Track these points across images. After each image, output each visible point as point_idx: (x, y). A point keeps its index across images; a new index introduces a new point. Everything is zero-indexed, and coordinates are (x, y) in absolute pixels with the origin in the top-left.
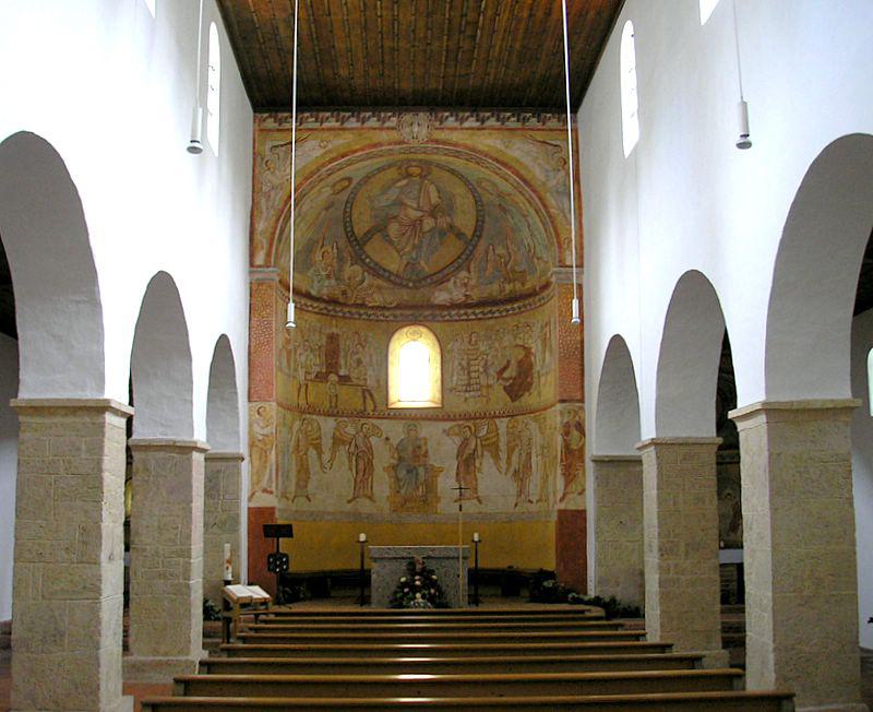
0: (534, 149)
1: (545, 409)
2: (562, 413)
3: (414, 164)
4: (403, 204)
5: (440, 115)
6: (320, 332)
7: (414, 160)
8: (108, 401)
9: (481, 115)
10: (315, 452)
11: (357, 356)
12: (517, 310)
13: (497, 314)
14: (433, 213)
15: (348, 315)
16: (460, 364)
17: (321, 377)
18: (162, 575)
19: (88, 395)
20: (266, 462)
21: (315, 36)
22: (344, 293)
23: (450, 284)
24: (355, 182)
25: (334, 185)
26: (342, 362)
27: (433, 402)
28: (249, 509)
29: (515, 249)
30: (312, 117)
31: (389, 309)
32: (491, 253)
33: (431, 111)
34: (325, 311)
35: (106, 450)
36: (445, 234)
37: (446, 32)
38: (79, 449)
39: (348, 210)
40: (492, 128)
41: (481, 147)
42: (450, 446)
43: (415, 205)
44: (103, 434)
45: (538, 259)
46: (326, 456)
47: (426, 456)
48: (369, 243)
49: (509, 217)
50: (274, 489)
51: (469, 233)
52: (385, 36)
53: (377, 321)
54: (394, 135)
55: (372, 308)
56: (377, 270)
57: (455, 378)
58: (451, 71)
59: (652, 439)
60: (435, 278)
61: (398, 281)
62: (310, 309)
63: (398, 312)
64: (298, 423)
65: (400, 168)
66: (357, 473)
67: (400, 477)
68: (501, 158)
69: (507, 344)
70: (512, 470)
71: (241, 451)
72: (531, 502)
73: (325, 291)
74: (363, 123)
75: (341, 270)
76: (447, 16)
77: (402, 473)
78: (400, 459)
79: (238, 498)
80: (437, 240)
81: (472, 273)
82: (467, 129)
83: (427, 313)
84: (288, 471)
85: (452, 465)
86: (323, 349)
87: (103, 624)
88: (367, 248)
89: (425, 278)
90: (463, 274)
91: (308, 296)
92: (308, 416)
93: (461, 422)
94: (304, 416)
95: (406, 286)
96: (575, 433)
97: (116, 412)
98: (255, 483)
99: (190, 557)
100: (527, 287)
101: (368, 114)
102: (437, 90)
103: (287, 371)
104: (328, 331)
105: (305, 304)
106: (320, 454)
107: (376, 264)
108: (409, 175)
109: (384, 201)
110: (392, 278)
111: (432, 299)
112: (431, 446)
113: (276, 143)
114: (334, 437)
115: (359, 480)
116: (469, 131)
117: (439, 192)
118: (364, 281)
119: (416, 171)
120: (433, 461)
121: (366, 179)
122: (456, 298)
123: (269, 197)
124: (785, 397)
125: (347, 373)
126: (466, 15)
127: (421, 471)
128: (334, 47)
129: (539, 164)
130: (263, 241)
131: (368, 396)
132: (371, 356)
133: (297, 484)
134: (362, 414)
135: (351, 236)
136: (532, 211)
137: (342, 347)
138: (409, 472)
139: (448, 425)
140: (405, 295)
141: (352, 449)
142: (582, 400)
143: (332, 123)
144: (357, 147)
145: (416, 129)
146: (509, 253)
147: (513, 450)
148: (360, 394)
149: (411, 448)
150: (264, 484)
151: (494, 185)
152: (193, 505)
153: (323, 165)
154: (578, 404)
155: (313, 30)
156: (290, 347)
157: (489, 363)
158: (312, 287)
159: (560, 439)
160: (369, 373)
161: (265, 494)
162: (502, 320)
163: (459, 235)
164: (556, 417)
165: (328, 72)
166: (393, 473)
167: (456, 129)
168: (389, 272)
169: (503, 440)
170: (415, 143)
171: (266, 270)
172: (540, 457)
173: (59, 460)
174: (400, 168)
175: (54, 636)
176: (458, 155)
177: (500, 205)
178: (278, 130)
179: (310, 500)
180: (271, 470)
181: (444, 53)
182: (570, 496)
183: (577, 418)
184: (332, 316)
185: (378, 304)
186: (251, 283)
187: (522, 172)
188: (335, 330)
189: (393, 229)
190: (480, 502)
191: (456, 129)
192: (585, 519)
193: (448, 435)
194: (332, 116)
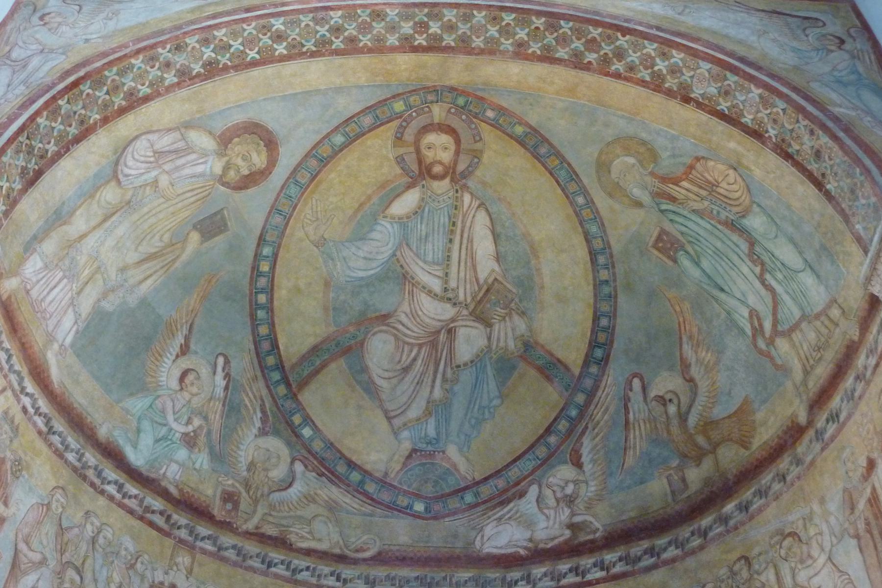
3: (438, 112)
4: (405, 279)
7: (437, 92)
12: (739, 517)
13: (672, 552)
14: (481, 317)
15: (231, 554)
23: (527, 505)
29: (708, 357)
31: (355, 562)
32: (636, 395)
34: (160, 521)
36: (514, 368)
43: (436, 285)
48: (313, 386)
51: (574, 357)
55: (309, 553)
60: (486, 491)
61: (385, 497)
62: (111, 489)
65: (404, 119)
75: (229, 434)
80: (492, 385)
81: (587, 467)
88: (309, 398)
89: (459, 491)
90: (565, 472)
95: (406, 511)
100: (756, 443)
105: (99, 474)
107: (330, 445)
110: (371, 488)
111: (478, 544)
117: (496, 237)
118: (290, 485)
129: (774, 40)
146: (691, 380)
158: (135, 446)
162: (690, 562)
168: (366, 473)
174: (399, 138)
184: (181, 541)
185: (323, 546)
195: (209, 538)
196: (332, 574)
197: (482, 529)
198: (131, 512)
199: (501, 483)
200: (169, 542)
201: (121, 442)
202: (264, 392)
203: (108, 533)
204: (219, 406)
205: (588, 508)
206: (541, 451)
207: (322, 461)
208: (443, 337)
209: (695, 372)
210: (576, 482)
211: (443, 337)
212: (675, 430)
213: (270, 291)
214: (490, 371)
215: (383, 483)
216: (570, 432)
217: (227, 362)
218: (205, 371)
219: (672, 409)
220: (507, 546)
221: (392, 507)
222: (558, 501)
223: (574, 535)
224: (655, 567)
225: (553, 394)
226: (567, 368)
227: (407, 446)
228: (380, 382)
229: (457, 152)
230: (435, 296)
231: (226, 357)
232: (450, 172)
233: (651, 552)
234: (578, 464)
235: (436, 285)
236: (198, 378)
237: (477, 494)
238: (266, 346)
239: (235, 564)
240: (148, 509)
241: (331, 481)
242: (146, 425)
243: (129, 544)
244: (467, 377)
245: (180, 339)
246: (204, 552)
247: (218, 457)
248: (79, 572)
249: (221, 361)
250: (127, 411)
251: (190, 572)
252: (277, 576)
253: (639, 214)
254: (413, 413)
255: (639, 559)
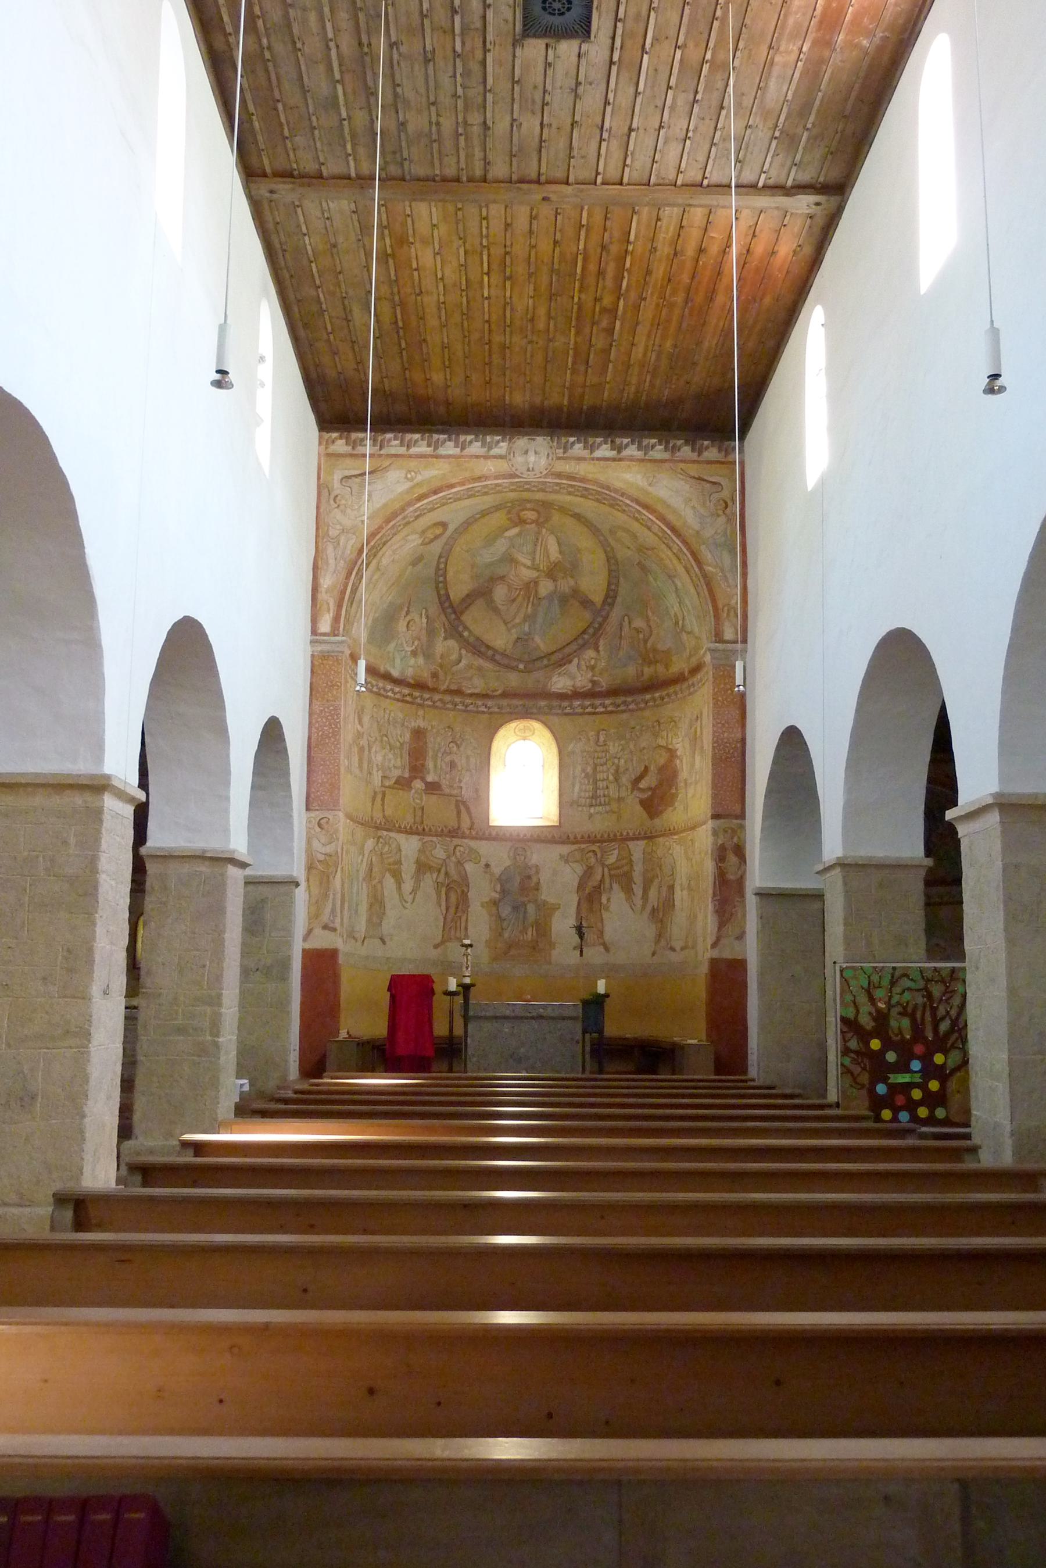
0: (687, 487)
1: (693, 828)
2: (715, 833)
5: (564, 440)
6: (403, 725)
7: (529, 501)
8: (108, 777)
9: (618, 441)
10: (392, 880)
11: (448, 759)
15: (438, 704)
16: (584, 770)
17: (403, 784)
18: (181, 1030)
19: (80, 767)
20: (328, 889)
21: (400, 324)
22: (435, 675)
23: (572, 667)
24: (451, 528)
25: (424, 532)
26: (430, 764)
27: (548, 819)
28: (304, 950)
30: (395, 439)
31: (492, 697)
33: (551, 435)
34: (408, 698)
35: (104, 845)
37: (573, 323)
38: (65, 843)
39: (442, 566)
40: (631, 459)
41: (618, 484)
42: (570, 875)
43: (529, 563)
44: (101, 821)
45: (689, 633)
46: (408, 886)
47: (537, 890)
49: (651, 579)
50: (337, 925)
51: (598, 598)
52: (493, 327)
53: (478, 712)
54: (503, 466)
55: (471, 695)
56: (479, 648)
57: (577, 789)
58: (580, 379)
59: (838, 858)
60: (554, 658)
61: (505, 661)
62: (390, 694)
63: (504, 702)
64: (370, 843)
66: (447, 909)
67: (503, 915)
68: (642, 498)
69: (644, 744)
70: (649, 908)
71: (295, 874)
72: (673, 949)
73: (410, 672)
74: (463, 449)
76: (576, 299)
77: (506, 911)
78: (504, 892)
79: (288, 931)
81: (602, 653)
82: (598, 459)
83: (543, 703)
84: (357, 905)
85: (572, 901)
86: (406, 747)
87: (92, 1082)
88: (464, 618)
90: (590, 653)
91: (387, 677)
92: (385, 833)
93: (583, 846)
94: (380, 833)
95: (515, 669)
96: (732, 859)
97: (121, 795)
98: (314, 916)
99: (220, 1005)
101: (470, 438)
102: (560, 409)
103: (357, 771)
104: (413, 724)
106: (399, 882)
107: (478, 639)
108: (522, 522)
109: (488, 556)
110: (498, 657)
112: (544, 877)
113: (347, 473)
114: (418, 862)
115: (449, 917)
116: (602, 463)
117: (559, 544)
118: (460, 661)
119: (530, 515)
120: (546, 895)
121: (467, 524)
122: (579, 684)
123: (339, 544)
124: (1029, 786)
125: (436, 779)
126: (600, 299)
127: (531, 909)
128: (424, 340)
129: (694, 508)
130: (328, 600)
131: (462, 808)
132: (468, 758)
133: (369, 921)
134: (454, 833)
135: (444, 601)
136: (681, 570)
137: (430, 745)
138: (516, 908)
139: (565, 849)
140: (513, 680)
141: (441, 878)
142: (742, 816)
143: (422, 448)
144: (454, 481)
145: (532, 458)
147: (652, 881)
148: (453, 807)
149: (518, 879)
150: (325, 918)
151: (634, 536)
152: (227, 935)
153: (410, 504)
154: (735, 821)
155: (399, 317)
156: (363, 742)
157: (621, 770)
158: (394, 667)
159: (709, 867)
160: (464, 781)
161: (327, 932)
163: (586, 603)
164: (704, 838)
165: (417, 376)
166: (494, 910)
167: (584, 459)
168: (495, 651)
169: (638, 869)
170: (530, 477)
171: (333, 639)
172: (685, 892)
173: (37, 857)
174: (509, 512)
175: (21, 1099)
176: (585, 494)
177: (638, 564)
178: (352, 455)
179: (384, 942)
180: (334, 899)
181: (571, 352)
182: (724, 941)
183: (735, 839)
184: (419, 705)
185: (476, 691)
186: (313, 656)
187: (670, 517)
188: (421, 723)
189: (500, 593)
190: (607, 949)
191: (584, 459)
192: (745, 970)
193: (567, 862)
194: (422, 440)
195: (428, 699)
196: (483, 705)
197: (551, 678)
198: (398, 700)
199: (559, 655)
200: (414, 707)
201: (389, 669)
202: (444, 619)
203: (392, 715)
204: (424, 632)
205: (601, 674)
206: (580, 641)
207: (474, 647)
208: (532, 584)
209: (652, 623)
210: (596, 659)
211: (532, 584)
212: (642, 645)
213: (445, 576)
214: (556, 602)
215: (504, 655)
216: (594, 634)
217: (427, 611)
218: (417, 618)
219: (641, 636)
220: (563, 688)
221: (507, 667)
222: (587, 667)
223: (593, 686)
224: (624, 711)
225: (587, 615)
226: (592, 603)
227: (515, 636)
228: (500, 607)
229: (539, 517)
230: (528, 567)
231: (426, 609)
232: (536, 522)
233: (624, 703)
234: (597, 650)
235: (529, 563)
236: (415, 622)
237: (549, 660)
238: (444, 598)
239: (440, 708)
240: (404, 696)
241: (479, 656)
242: (396, 654)
243: (400, 715)
244: (545, 603)
245: (406, 609)
246: (429, 706)
247: (428, 656)
248: (386, 736)
249: (424, 611)
250: (389, 652)
251: (424, 718)
252: (459, 710)
253: (630, 553)
254: (517, 621)
255: (619, 706)
